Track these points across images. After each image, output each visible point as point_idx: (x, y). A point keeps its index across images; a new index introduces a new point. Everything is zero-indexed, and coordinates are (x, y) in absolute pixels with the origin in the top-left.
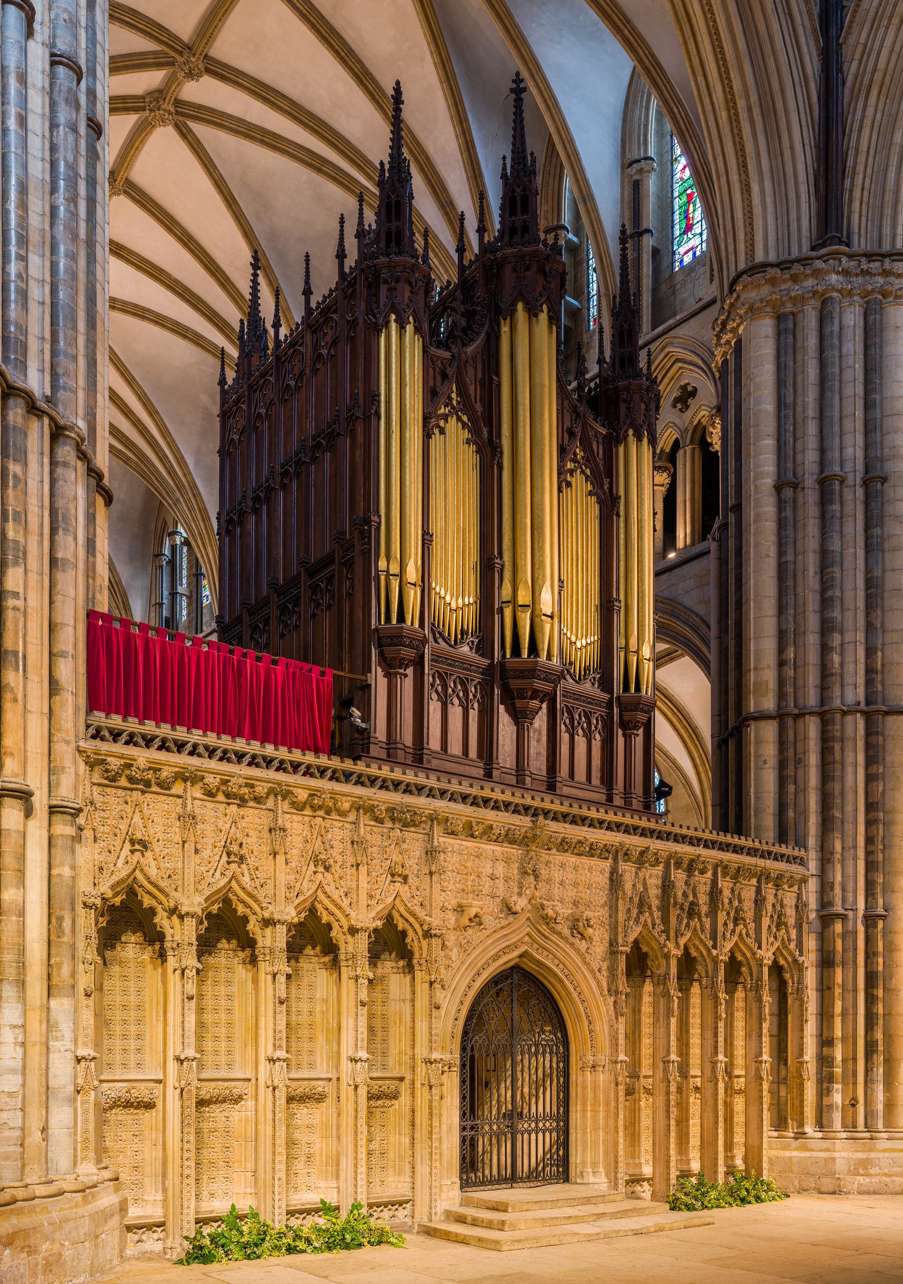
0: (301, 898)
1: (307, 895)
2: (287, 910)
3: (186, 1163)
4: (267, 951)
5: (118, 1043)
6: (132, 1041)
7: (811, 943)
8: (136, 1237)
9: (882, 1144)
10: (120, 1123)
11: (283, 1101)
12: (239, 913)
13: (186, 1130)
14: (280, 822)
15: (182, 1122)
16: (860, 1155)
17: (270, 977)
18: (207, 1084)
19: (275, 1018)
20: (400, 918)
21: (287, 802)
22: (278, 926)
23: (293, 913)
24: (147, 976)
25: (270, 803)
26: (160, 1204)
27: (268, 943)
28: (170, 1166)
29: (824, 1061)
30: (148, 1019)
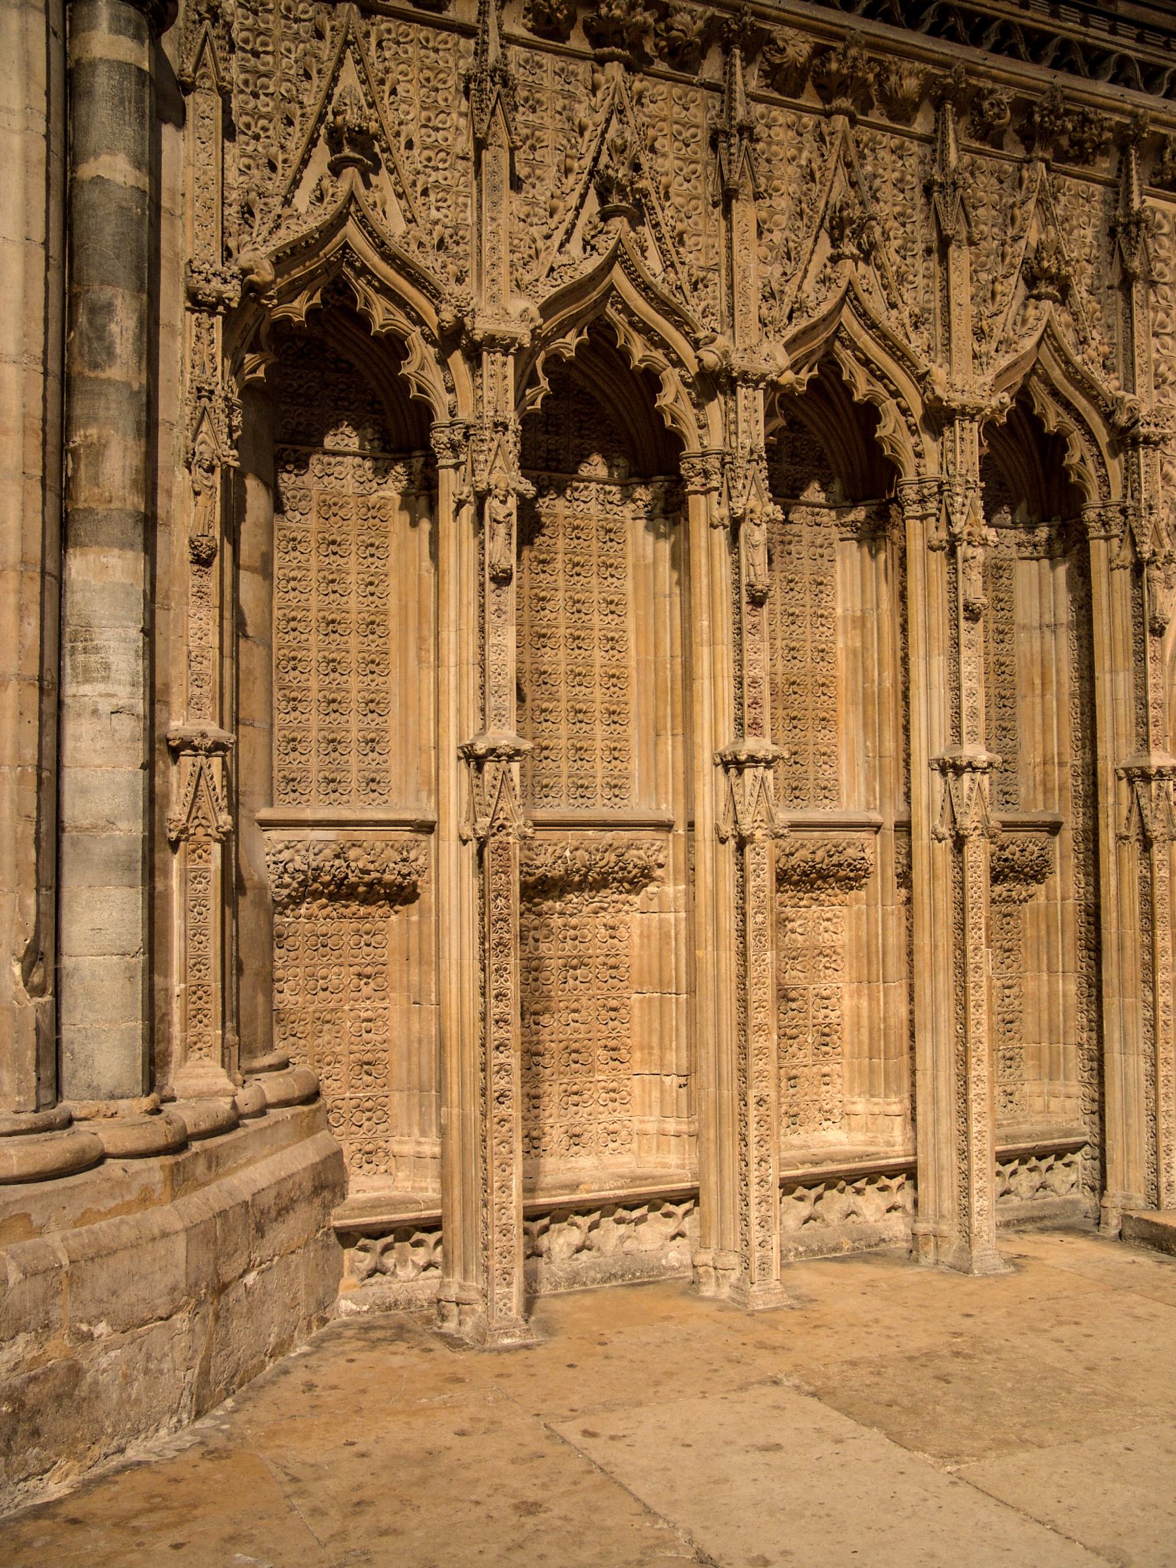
0: (803, 323)
1: (817, 315)
2: (765, 348)
3: (498, 1058)
4: (714, 463)
6: (354, 718)
8: (367, 1261)
10: (322, 943)
11: (767, 878)
12: (635, 362)
13: (493, 962)
14: (740, 113)
15: (483, 939)
17: (721, 535)
18: (555, 835)
19: (739, 647)
21: (755, 70)
22: (741, 392)
23: (783, 359)
24: (393, 542)
25: (711, 70)
26: (433, 1167)
27: (715, 440)
28: (453, 1063)
30: (394, 657)
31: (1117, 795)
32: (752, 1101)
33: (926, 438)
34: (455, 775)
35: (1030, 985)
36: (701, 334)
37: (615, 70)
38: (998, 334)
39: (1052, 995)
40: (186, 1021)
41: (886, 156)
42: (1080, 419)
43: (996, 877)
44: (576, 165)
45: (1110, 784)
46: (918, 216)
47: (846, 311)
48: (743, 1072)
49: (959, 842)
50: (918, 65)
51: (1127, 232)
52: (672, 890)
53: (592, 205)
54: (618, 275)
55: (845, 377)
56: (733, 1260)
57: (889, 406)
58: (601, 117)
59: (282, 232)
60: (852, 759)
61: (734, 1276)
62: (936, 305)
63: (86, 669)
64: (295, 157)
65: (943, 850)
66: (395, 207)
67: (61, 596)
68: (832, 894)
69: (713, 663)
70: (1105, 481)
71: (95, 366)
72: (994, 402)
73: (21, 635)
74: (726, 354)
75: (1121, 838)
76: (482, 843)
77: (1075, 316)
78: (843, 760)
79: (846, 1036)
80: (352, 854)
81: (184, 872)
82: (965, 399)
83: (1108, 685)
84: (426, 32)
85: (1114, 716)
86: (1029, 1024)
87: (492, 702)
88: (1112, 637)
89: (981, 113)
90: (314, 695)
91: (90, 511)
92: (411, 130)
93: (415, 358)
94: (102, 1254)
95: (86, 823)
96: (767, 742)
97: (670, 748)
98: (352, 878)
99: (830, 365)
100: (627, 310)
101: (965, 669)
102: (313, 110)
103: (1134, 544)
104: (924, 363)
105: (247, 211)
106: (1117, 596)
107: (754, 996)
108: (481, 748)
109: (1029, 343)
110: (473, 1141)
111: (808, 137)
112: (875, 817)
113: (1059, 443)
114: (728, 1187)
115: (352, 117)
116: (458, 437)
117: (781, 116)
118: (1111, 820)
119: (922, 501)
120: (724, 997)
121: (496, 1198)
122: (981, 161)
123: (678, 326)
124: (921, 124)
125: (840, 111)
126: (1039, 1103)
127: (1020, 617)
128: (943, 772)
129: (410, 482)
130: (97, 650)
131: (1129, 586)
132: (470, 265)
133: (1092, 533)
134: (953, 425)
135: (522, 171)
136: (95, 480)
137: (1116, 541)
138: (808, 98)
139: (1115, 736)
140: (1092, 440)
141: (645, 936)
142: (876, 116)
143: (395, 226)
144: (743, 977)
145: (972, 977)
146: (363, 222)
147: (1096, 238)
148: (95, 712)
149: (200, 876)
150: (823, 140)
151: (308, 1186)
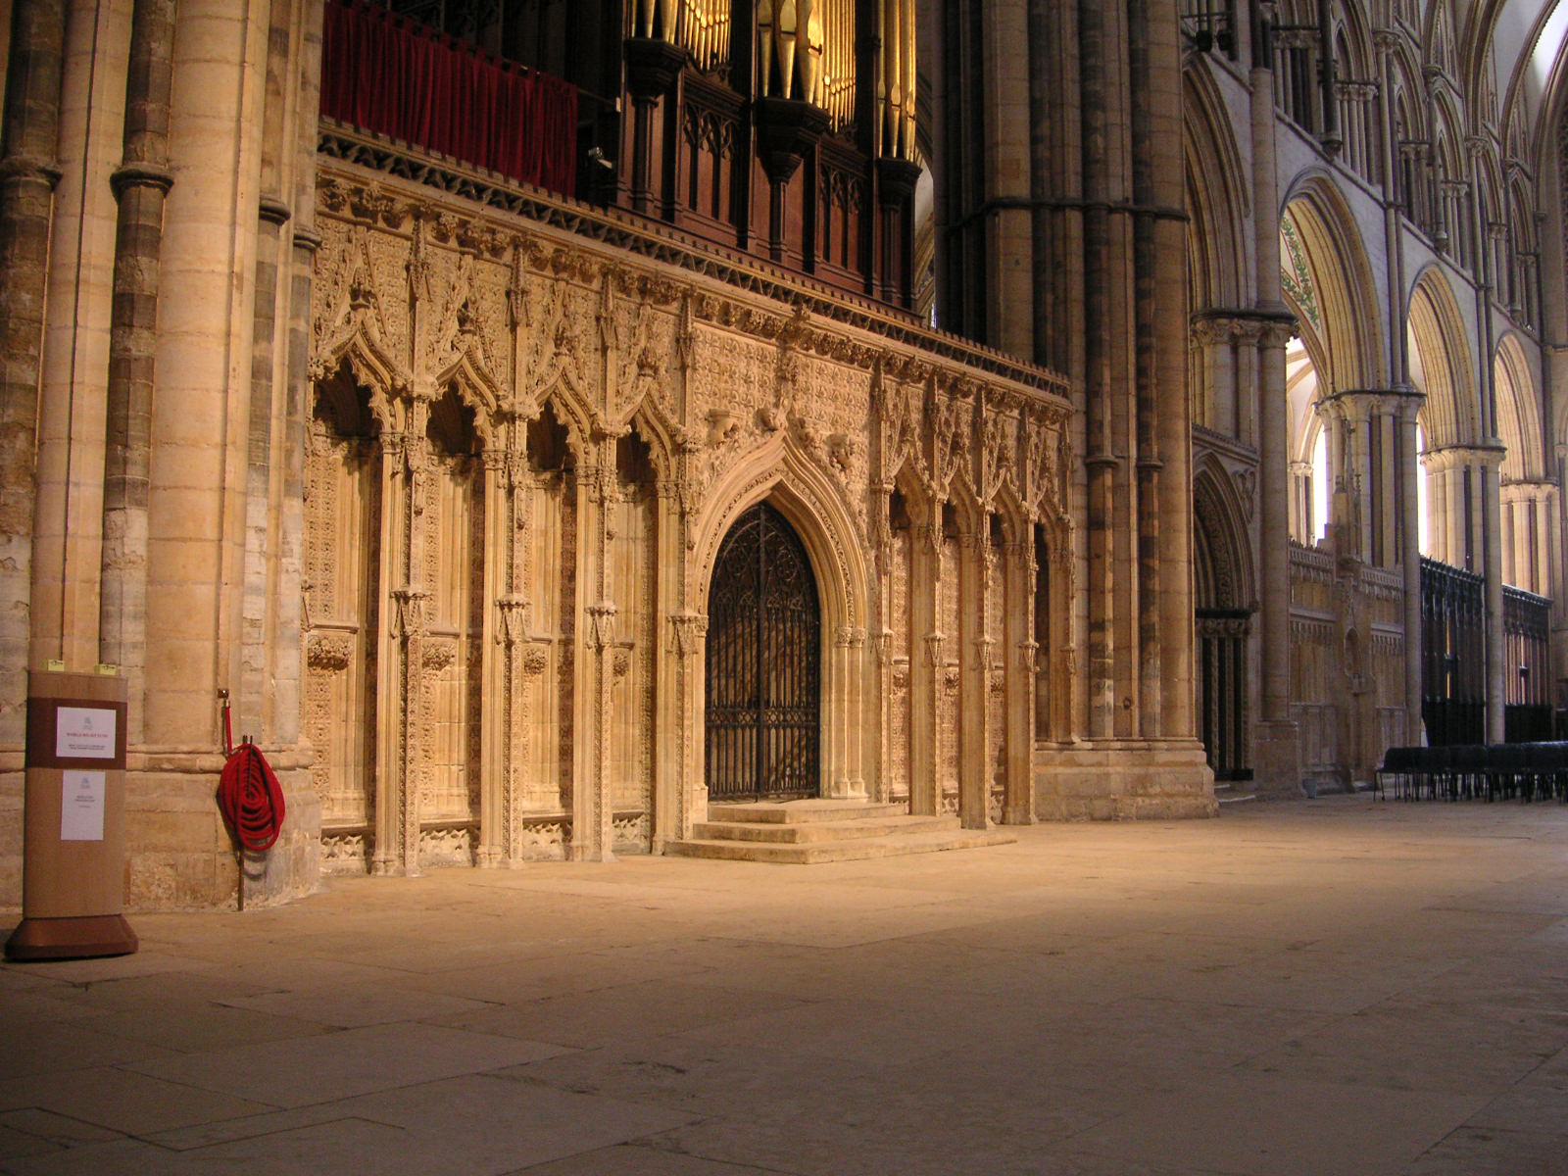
6: (319, 572)
7: (1076, 498)
9: (1162, 757)
16: (1137, 770)
20: (644, 425)
24: (339, 482)
29: (1093, 649)
31: (667, 630)
32: (512, 771)
33: (591, 445)
36: (500, 393)
37: (469, 259)
41: (579, 300)
42: (658, 436)
49: (600, 649)
50: (599, 259)
51: (685, 343)
55: (555, 411)
56: (498, 849)
57: (573, 427)
61: (499, 857)
65: (591, 653)
69: (495, 556)
70: (668, 468)
72: (624, 431)
74: (513, 405)
75: (668, 652)
77: (660, 384)
80: (323, 642)
85: (667, 590)
89: (624, 281)
96: (522, 596)
98: (323, 655)
100: (467, 378)
103: (681, 503)
106: (671, 528)
109: (639, 399)
111: (547, 290)
113: (647, 447)
114: (496, 814)
117: (536, 280)
119: (587, 476)
120: (497, 720)
122: (621, 303)
123: (489, 387)
125: (563, 280)
128: (592, 614)
129: (349, 452)
139: (667, 600)
145: (604, 717)
147: (670, 343)
150: (554, 293)
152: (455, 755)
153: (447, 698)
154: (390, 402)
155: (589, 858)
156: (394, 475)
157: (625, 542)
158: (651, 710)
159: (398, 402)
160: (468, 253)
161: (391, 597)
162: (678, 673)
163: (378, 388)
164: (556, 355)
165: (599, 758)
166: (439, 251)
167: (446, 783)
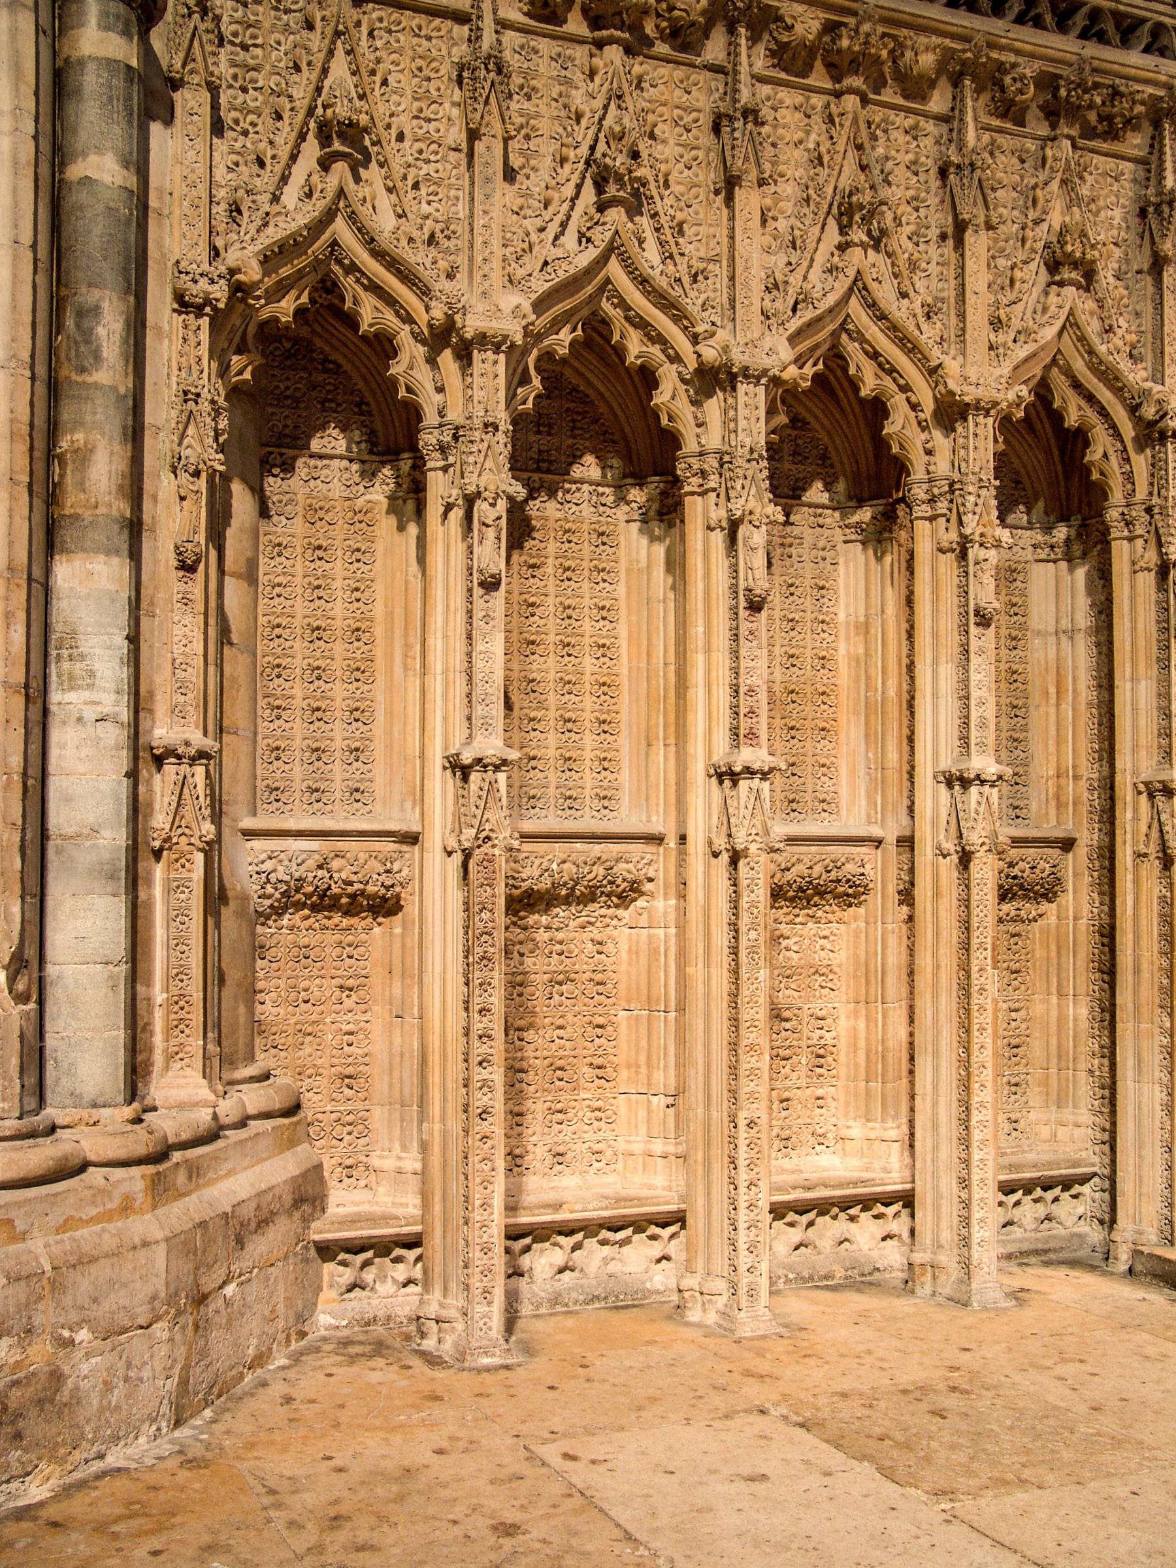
0: (806, 314)
1: (823, 306)
2: (768, 342)
3: (479, 1074)
4: (712, 462)
5: (298, 731)
6: (338, 726)
8: (347, 1276)
10: (304, 955)
11: (762, 894)
12: (630, 359)
13: (477, 976)
14: (745, 96)
15: (467, 953)
17: (718, 539)
18: (542, 847)
19: (735, 654)
21: (760, 49)
22: (742, 388)
23: (786, 353)
24: (380, 547)
25: (715, 49)
26: (414, 1183)
27: (713, 439)
28: (435, 1078)
30: (380, 664)
31: (1136, 810)
32: (742, 1123)
33: (937, 434)
34: (441, 785)
35: (1038, 1009)
36: (700, 329)
37: (614, 53)
38: (1016, 324)
39: (1061, 1019)
40: (168, 1030)
41: (898, 137)
42: (1103, 413)
43: (1004, 896)
44: (572, 154)
45: (1129, 798)
46: (933, 200)
47: (854, 301)
48: (733, 1093)
49: (965, 859)
50: (935, 40)
51: (1159, 213)
52: (661, 904)
53: (589, 195)
54: (614, 268)
55: (852, 371)
56: (720, 1285)
57: (898, 402)
58: (598, 103)
59: (270, 230)
60: (852, 771)
61: (721, 1302)
62: (951, 293)
63: (71, 677)
64: (284, 153)
65: (948, 868)
66: (385, 202)
67: (47, 603)
68: (830, 911)
69: (708, 671)
70: (1129, 478)
71: (82, 370)
72: (1011, 396)
73: (8, 642)
74: (726, 349)
76: (467, 855)
77: (1101, 303)
78: (844, 772)
79: (842, 1058)
80: (335, 864)
81: (167, 881)
82: (980, 392)
83: (1128, 694)
84: (420, 19)
85: (1135, 727)
86: (1036, 1049)
87: (479, 710)
88: (1134, 644)
89: (1003, 89)
90: (298, 703)
91: (76, 517)
92: (403, 122)
93: (404, 357)
94: (84, 1261)
95: (69, 830)
96: (763, 753)
97: (662, 759)
98: (335, 890)
99: (836, 358)
100: (623, 305)
101: (974, 677)
102: (302, 104)
103: (1160, 545)
104: (936, 355)
105: (235, 209)
106: (1140, 600)
107: (745, 1015)
108: (467, 758)
109: (1049, 333)
110: (455, 1157)
111: (817, 118)
112: (876, 831)
113: (1080, 438)
114: (715, 1211)
115: (342, 111)
116: (447, 438)
117: (788, 97)
118: (1129, 836)
119: (932, 501)
120: (715, 1015)
121: (477, 1215)
122: (1001, 139)
123: (676, 320)
124: (938, 102)
125: (851, 91)
126: (1045, 1132)
127: (1034, 622)
128: (950, 785)
129: (398, 485)
130: (82, 657)
131: (1153, 589)
132: (462, 260)
133: (1114, 533)
134: (966, 420)
135: (516, 161)
136: (82, 486)
137: (1140, 542)
138: (819, 78)
139: (1135, 748)
140: (1117, 434)
141: (634, 952)
142: (889, 95)
143: (384, 222)
144: (734, 996)
145: (976, 999)
146: (353, 217)
147: (1125, 220)
148: (80, 720)
149: (183, 885)
150: (832, 122)
151: (288, 1199)
152: (659, 1076)
153: (643, 960)
154: (432, 361)
155: (947, 1291)
156: (449, 508)
157: (1052, 640)
158: (1108, 971)
159: (447, 357)
160: (611, 41)
161: (445, 768)
162: (1162, 898)
163: (404, 336)
164: (842, 248)
165: (966, 1085)
166: (543, 44)
167: (643, 1130)
